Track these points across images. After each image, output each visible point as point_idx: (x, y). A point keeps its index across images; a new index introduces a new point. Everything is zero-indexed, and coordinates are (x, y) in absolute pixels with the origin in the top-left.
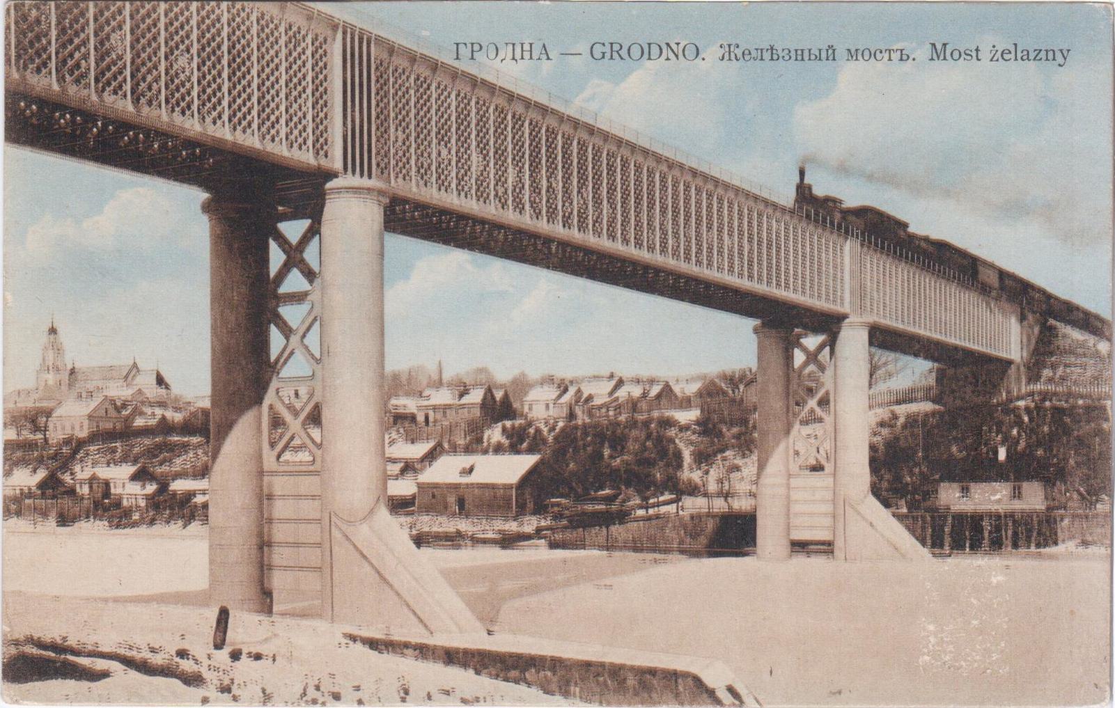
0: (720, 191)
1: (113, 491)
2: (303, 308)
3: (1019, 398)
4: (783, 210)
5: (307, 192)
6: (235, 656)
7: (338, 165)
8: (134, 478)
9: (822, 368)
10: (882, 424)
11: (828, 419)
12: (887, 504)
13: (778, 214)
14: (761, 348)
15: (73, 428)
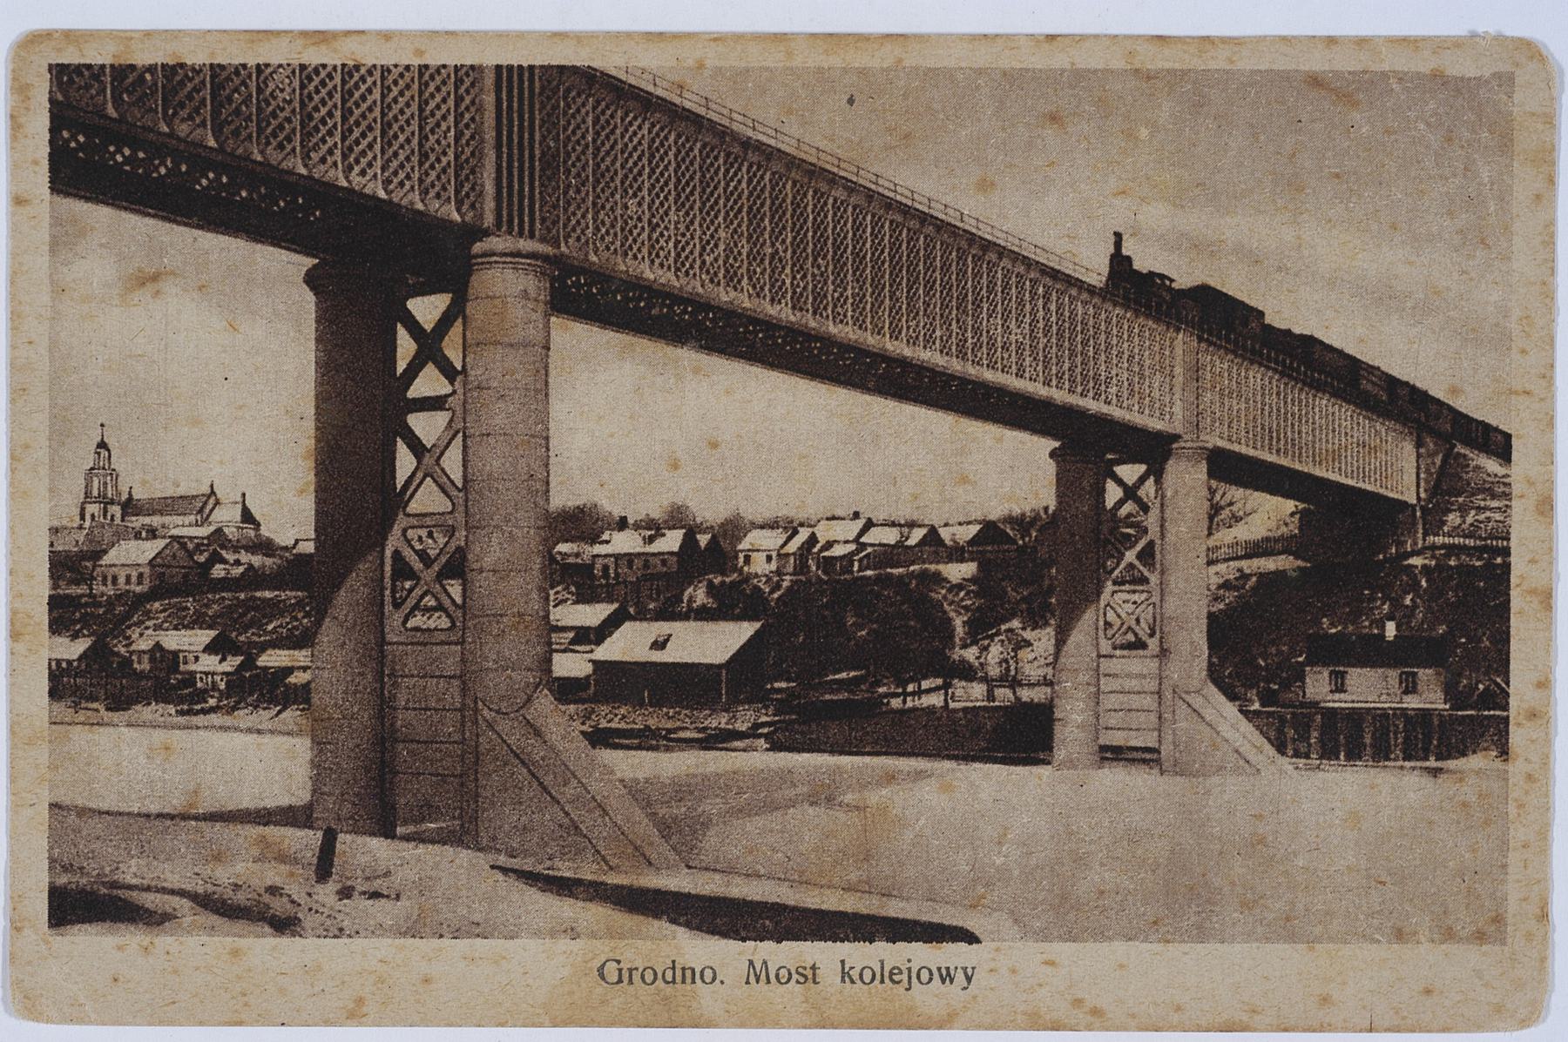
0: (1005, 262)
1: (182, 668)
2: (441, 418)
3: (1415, 553)
4: (1091, 290)
5: (446, 259)
6: (346, 893)
7: (489, 220)
8: (210, 649)
9: (1145, 508)
10: (1226, 585)
11: (1154, 579)
12: (1232, 697)
13: (1085, 296)
14: (1061, 480)
15: (128, 581)
